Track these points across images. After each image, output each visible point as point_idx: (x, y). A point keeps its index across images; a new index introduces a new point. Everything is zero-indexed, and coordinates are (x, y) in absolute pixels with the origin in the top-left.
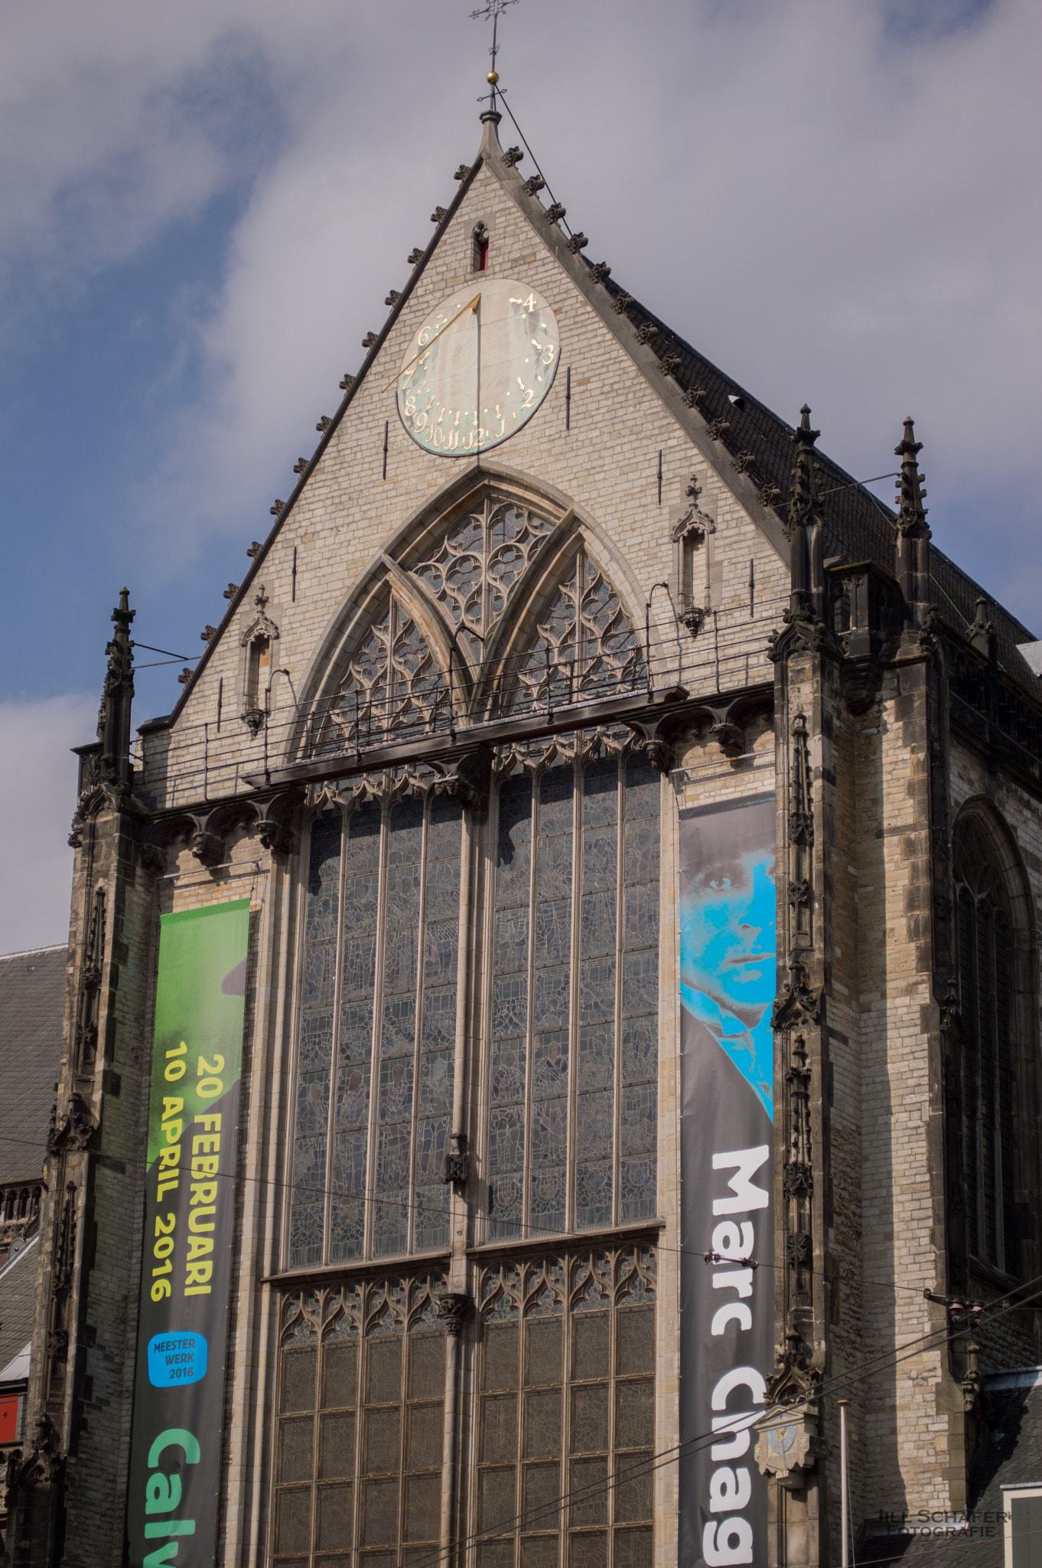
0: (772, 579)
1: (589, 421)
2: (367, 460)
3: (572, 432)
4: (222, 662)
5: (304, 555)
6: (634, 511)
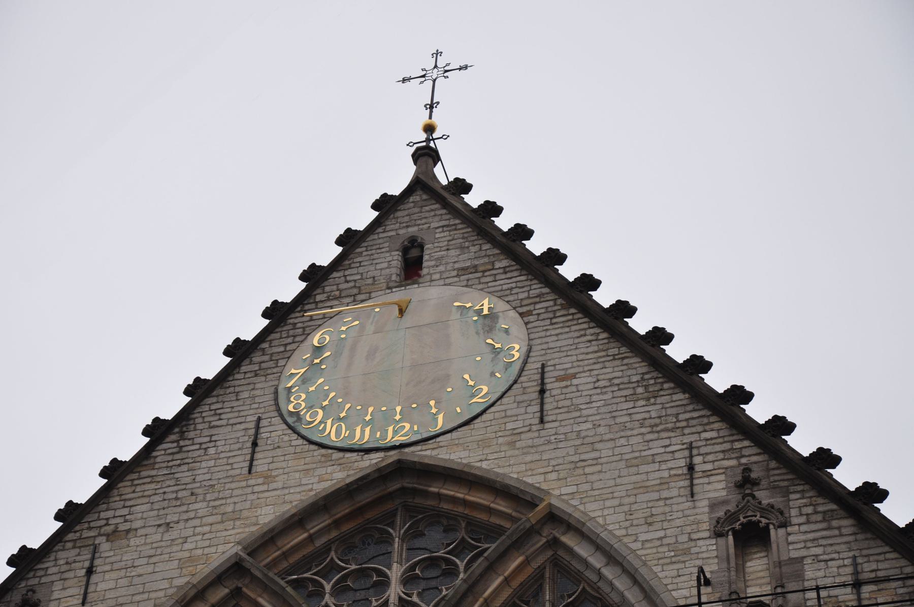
1: (578, 414)
3: (547, 426)
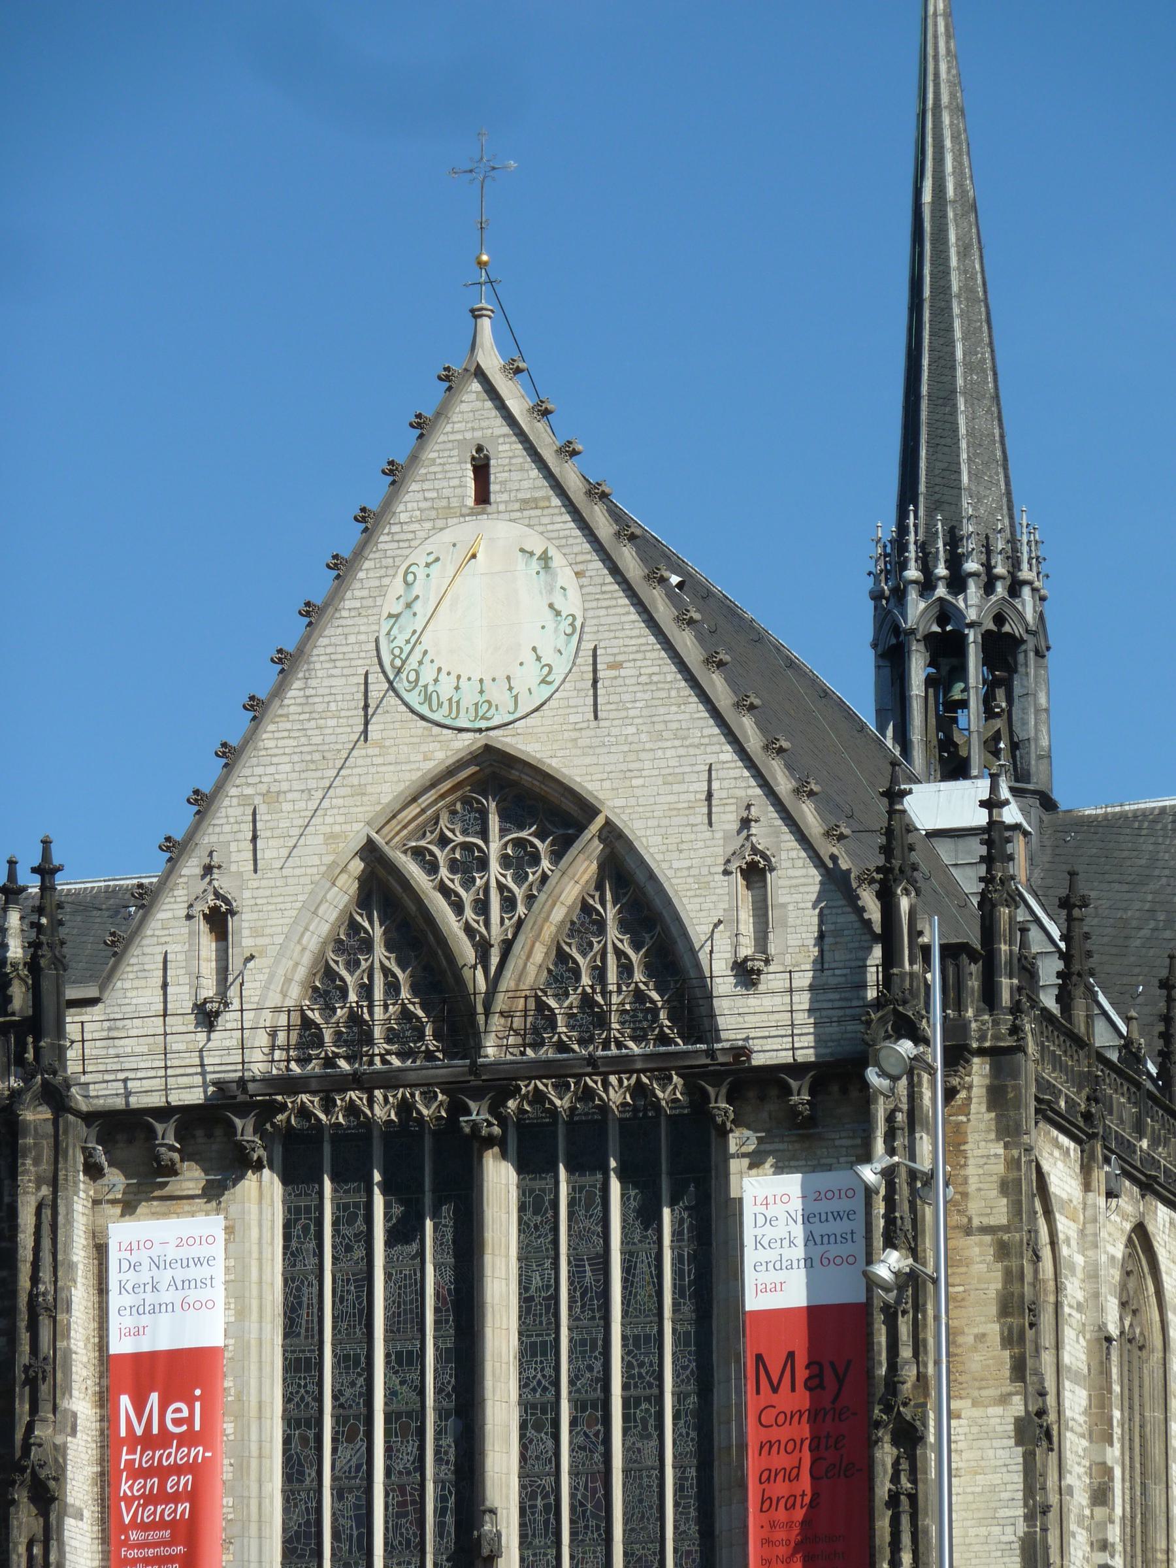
0: (846, 932)
1: (624, 714)
2: (343, 714)
3: (602, 723)
4: (166, 932)
5: (268, 817)
6: (681, 830)
